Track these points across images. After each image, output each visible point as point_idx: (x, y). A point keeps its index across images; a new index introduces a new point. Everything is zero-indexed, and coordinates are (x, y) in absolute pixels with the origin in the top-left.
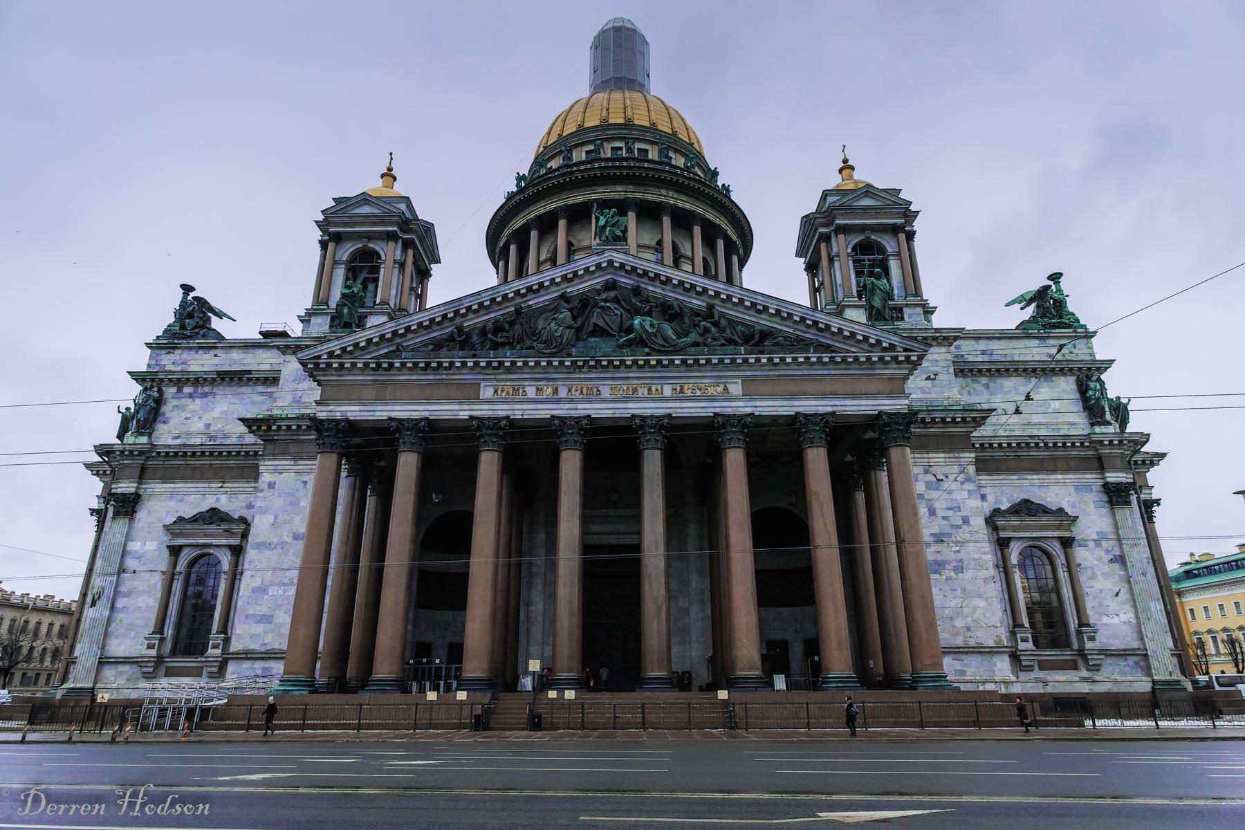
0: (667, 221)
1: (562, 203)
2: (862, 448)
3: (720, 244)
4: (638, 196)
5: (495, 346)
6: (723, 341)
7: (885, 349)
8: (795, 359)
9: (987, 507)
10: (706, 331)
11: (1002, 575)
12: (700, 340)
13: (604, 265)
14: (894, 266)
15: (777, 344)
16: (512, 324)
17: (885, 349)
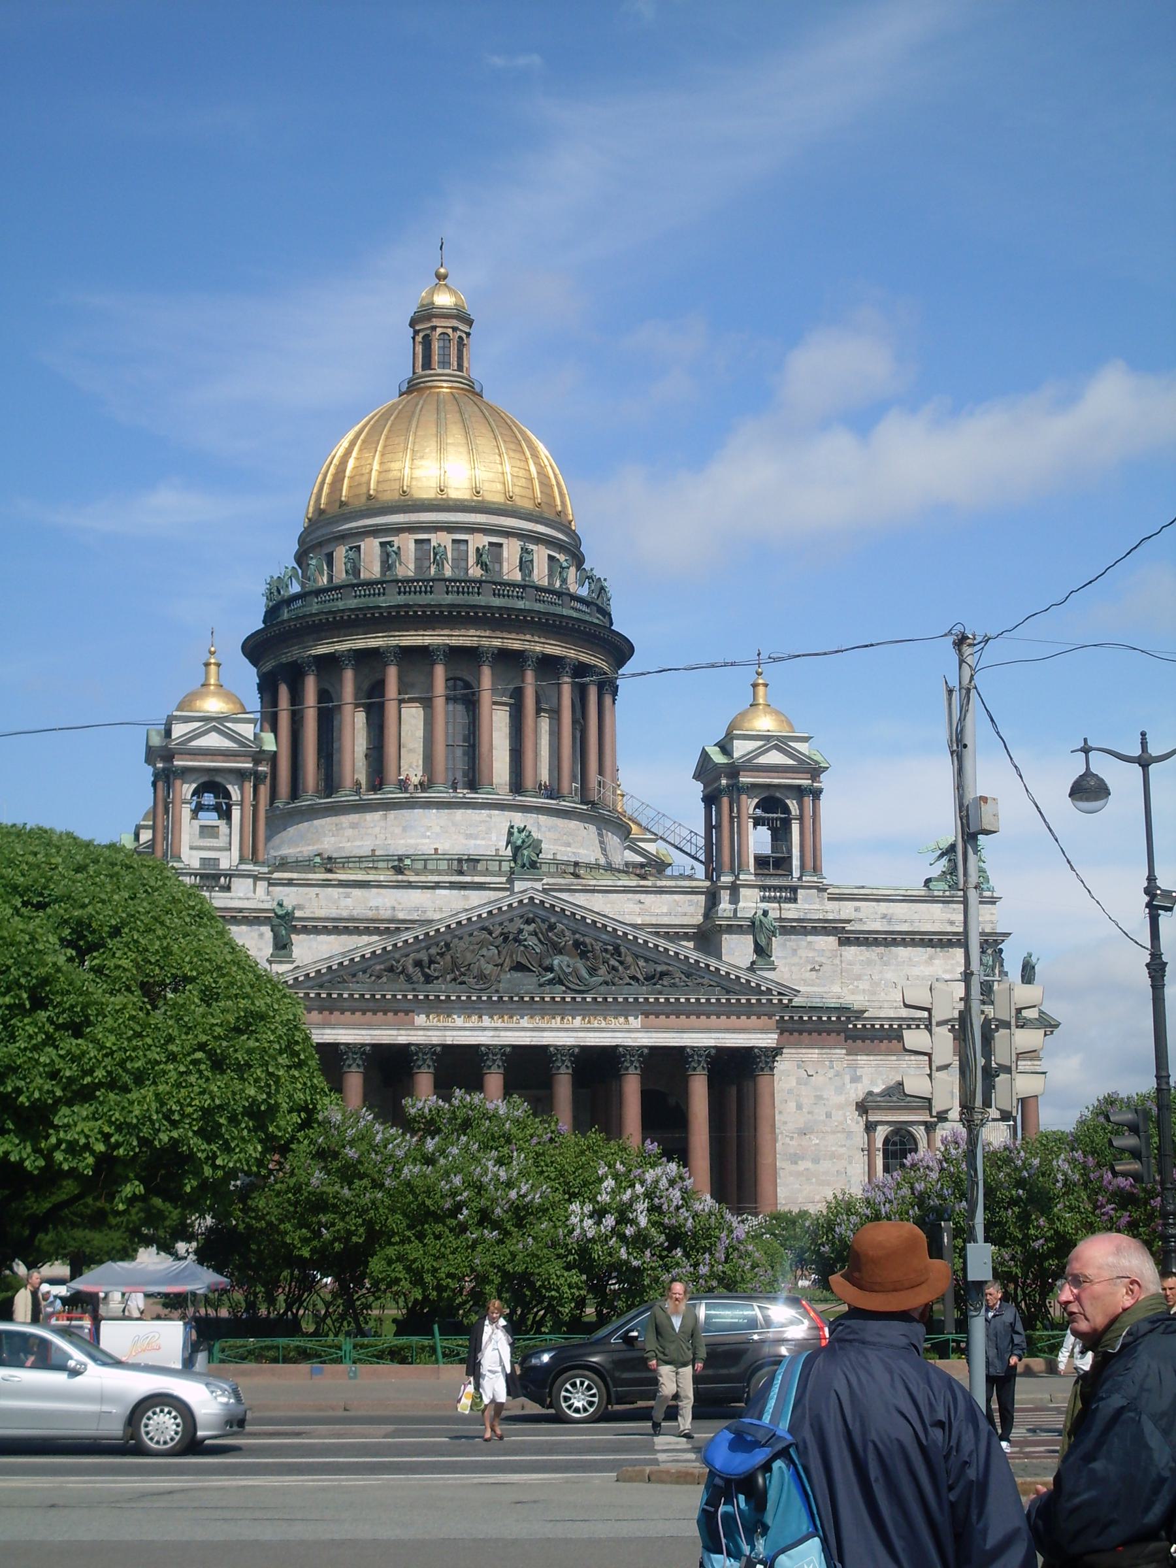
0: (530, 676)
1: (393, 642)
2: (738, 1073)
3: (593, 693)
4: (497, 643)
5: (428, 979)
6: (628, 980)
7: (762, 993)
8: (688, 1000)
9: (857, 1092)
10: (614, 969)
11: (866, 1158)
12: (608, 978)
13: (526, 901)
14: (795, 827)
15: (674, 985)
16: (442, 955)
17: (762, 993)
